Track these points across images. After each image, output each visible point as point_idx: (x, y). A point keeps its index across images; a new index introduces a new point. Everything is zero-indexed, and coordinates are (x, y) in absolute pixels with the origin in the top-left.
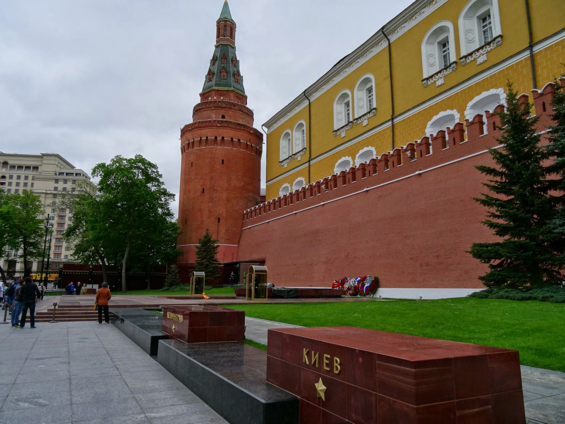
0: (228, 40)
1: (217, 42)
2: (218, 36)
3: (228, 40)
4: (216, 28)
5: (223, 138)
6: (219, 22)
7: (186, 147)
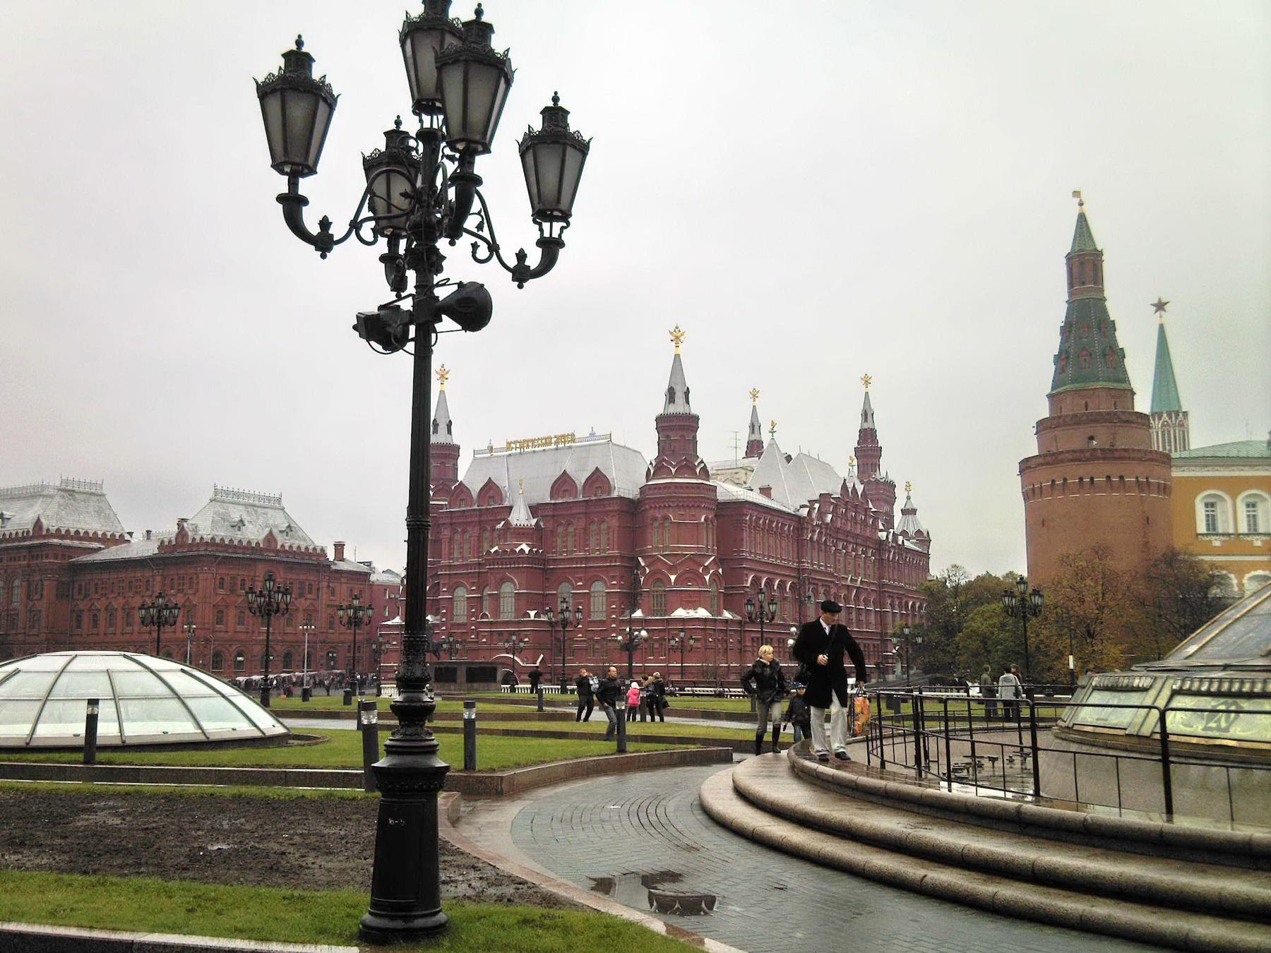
0: (1089, 290)
1: (1071, 294)
2: (1071, 284)
3: (1089, 290)
4: (1065, 269)
5: (1092, 479)
6: (1069, 258)
7: (1030, 494)
